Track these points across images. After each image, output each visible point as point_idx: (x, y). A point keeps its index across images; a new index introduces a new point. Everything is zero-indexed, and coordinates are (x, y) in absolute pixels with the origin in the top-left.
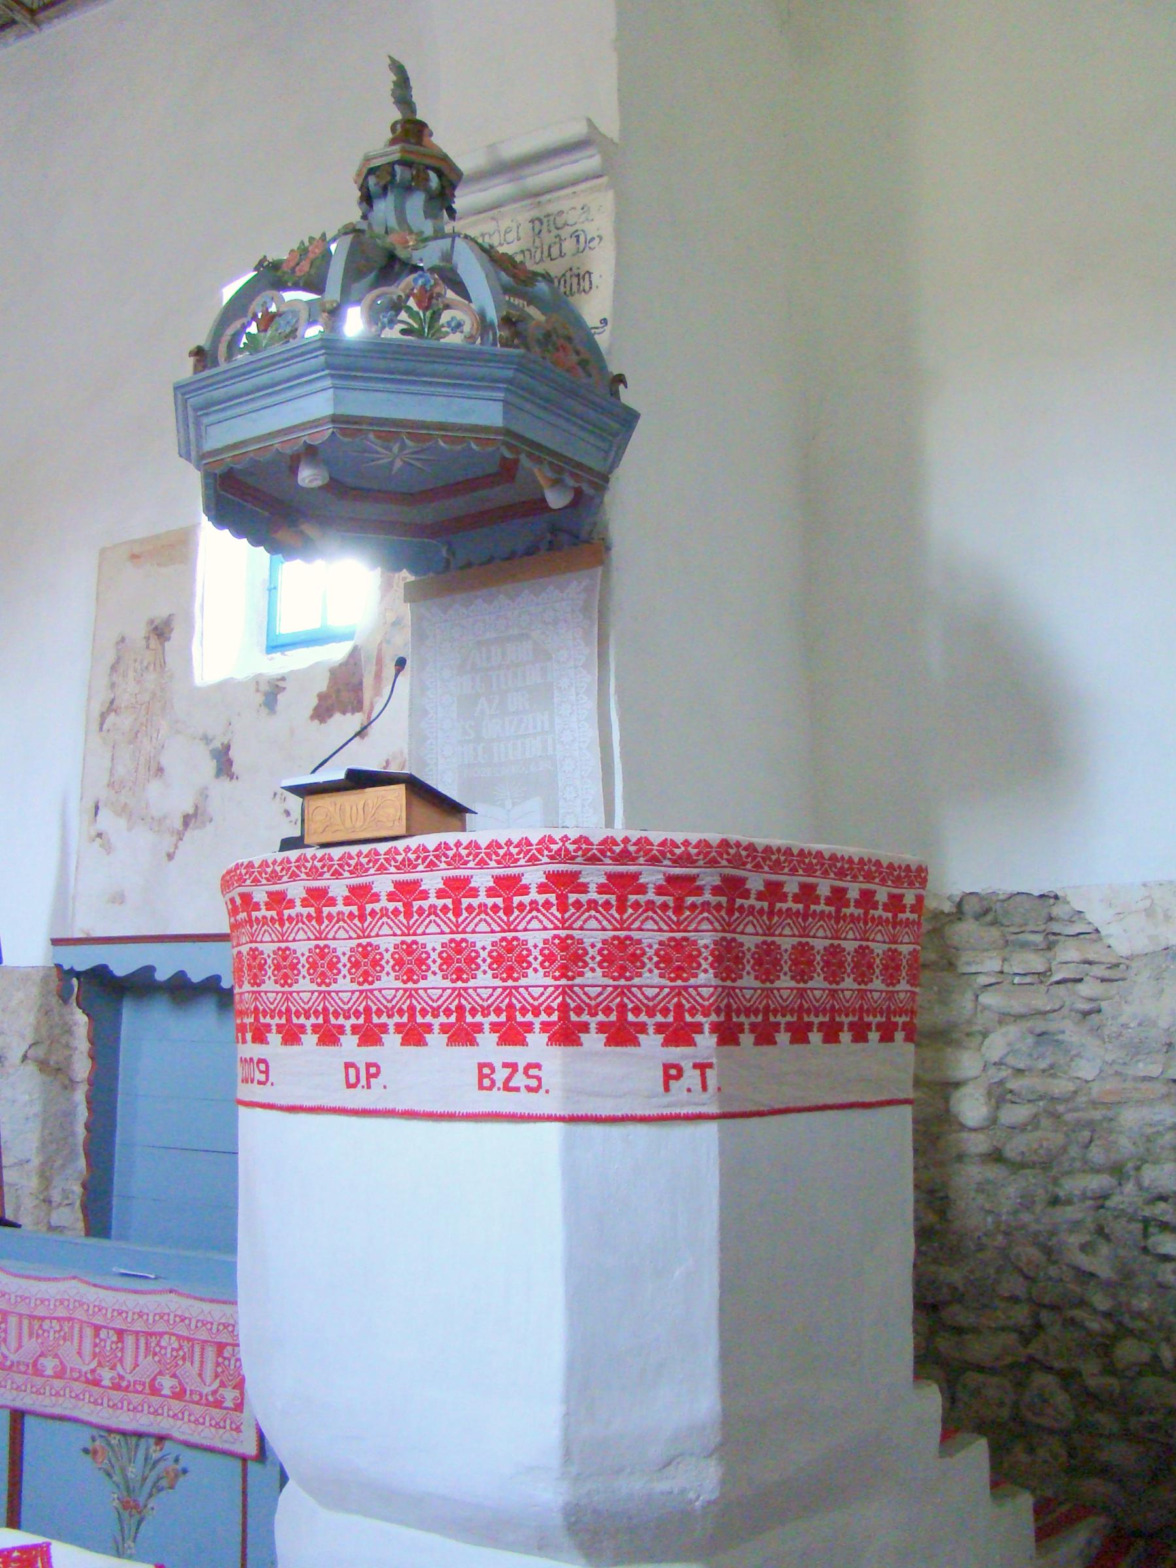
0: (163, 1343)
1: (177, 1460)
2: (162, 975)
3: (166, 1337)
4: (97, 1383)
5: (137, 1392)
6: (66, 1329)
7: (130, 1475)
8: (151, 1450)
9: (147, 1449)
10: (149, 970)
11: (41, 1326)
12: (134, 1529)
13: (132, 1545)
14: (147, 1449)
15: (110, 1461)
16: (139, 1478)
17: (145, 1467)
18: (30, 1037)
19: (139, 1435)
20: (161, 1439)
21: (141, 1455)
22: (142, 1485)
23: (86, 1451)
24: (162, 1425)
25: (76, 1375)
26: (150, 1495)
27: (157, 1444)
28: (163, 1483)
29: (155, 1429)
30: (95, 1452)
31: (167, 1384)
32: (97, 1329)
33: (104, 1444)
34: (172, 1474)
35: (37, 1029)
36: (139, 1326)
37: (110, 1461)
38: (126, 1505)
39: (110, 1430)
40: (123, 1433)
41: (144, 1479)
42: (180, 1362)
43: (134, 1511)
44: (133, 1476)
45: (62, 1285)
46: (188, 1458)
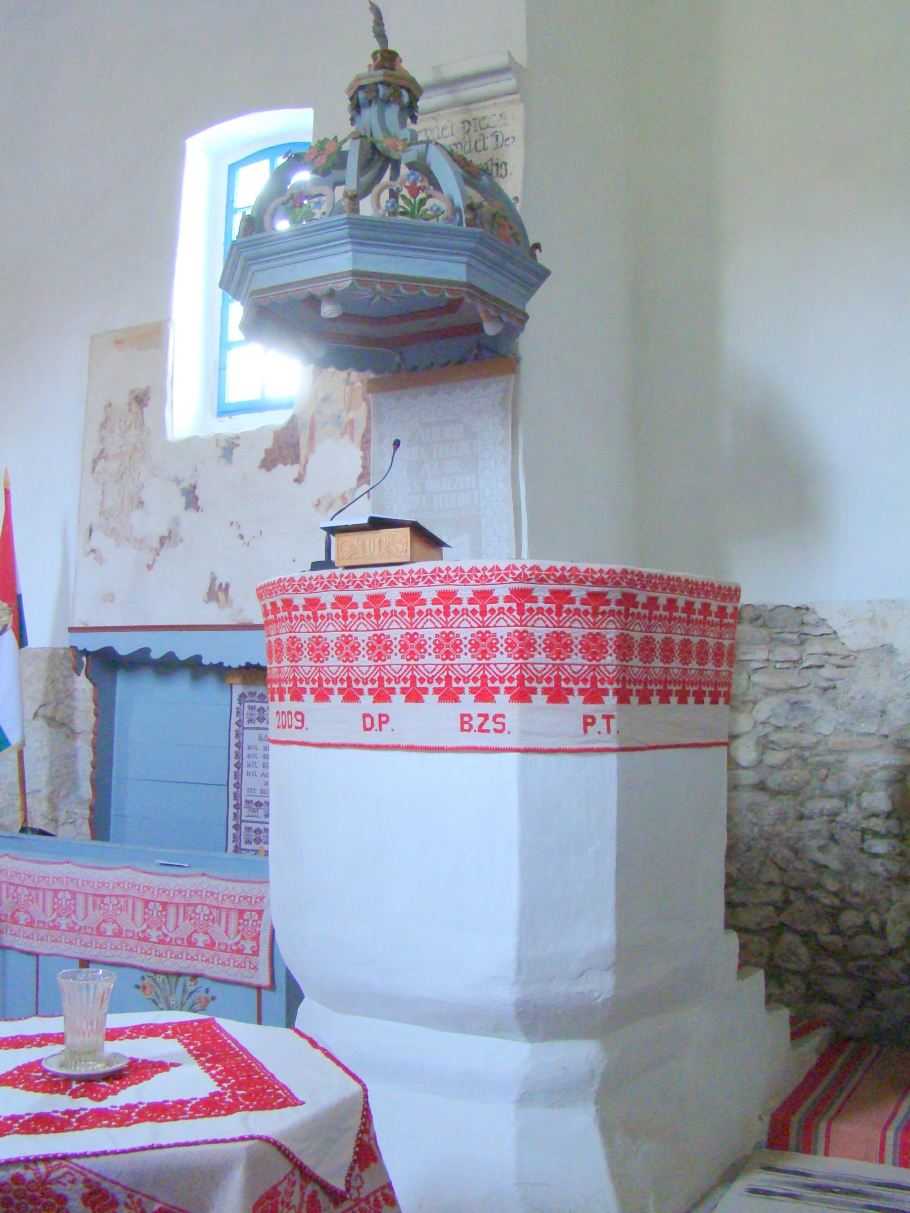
0: (197, 911)
1: (207, 991)
3: (200, 907)
4: (146, 939)
6: (122, 903)
11: (102, 902)
14: (185, 985)
15: (156, 993)
19: (179, 975)
20: (195, 977)
21: (180, 989)
23: (138, 987)
25: (130, 934)
27: (192, 980)
29: (192, 970)
30: (144, 988)
31: (201, 939)
32: (147, 902)
33: (152, 982)
34: (203, 1000)
37: (156, 993)
39: (156, 972)
40: (166, 974)
44: (174, 1003)
45: (119, 873)
46: (216, 988)
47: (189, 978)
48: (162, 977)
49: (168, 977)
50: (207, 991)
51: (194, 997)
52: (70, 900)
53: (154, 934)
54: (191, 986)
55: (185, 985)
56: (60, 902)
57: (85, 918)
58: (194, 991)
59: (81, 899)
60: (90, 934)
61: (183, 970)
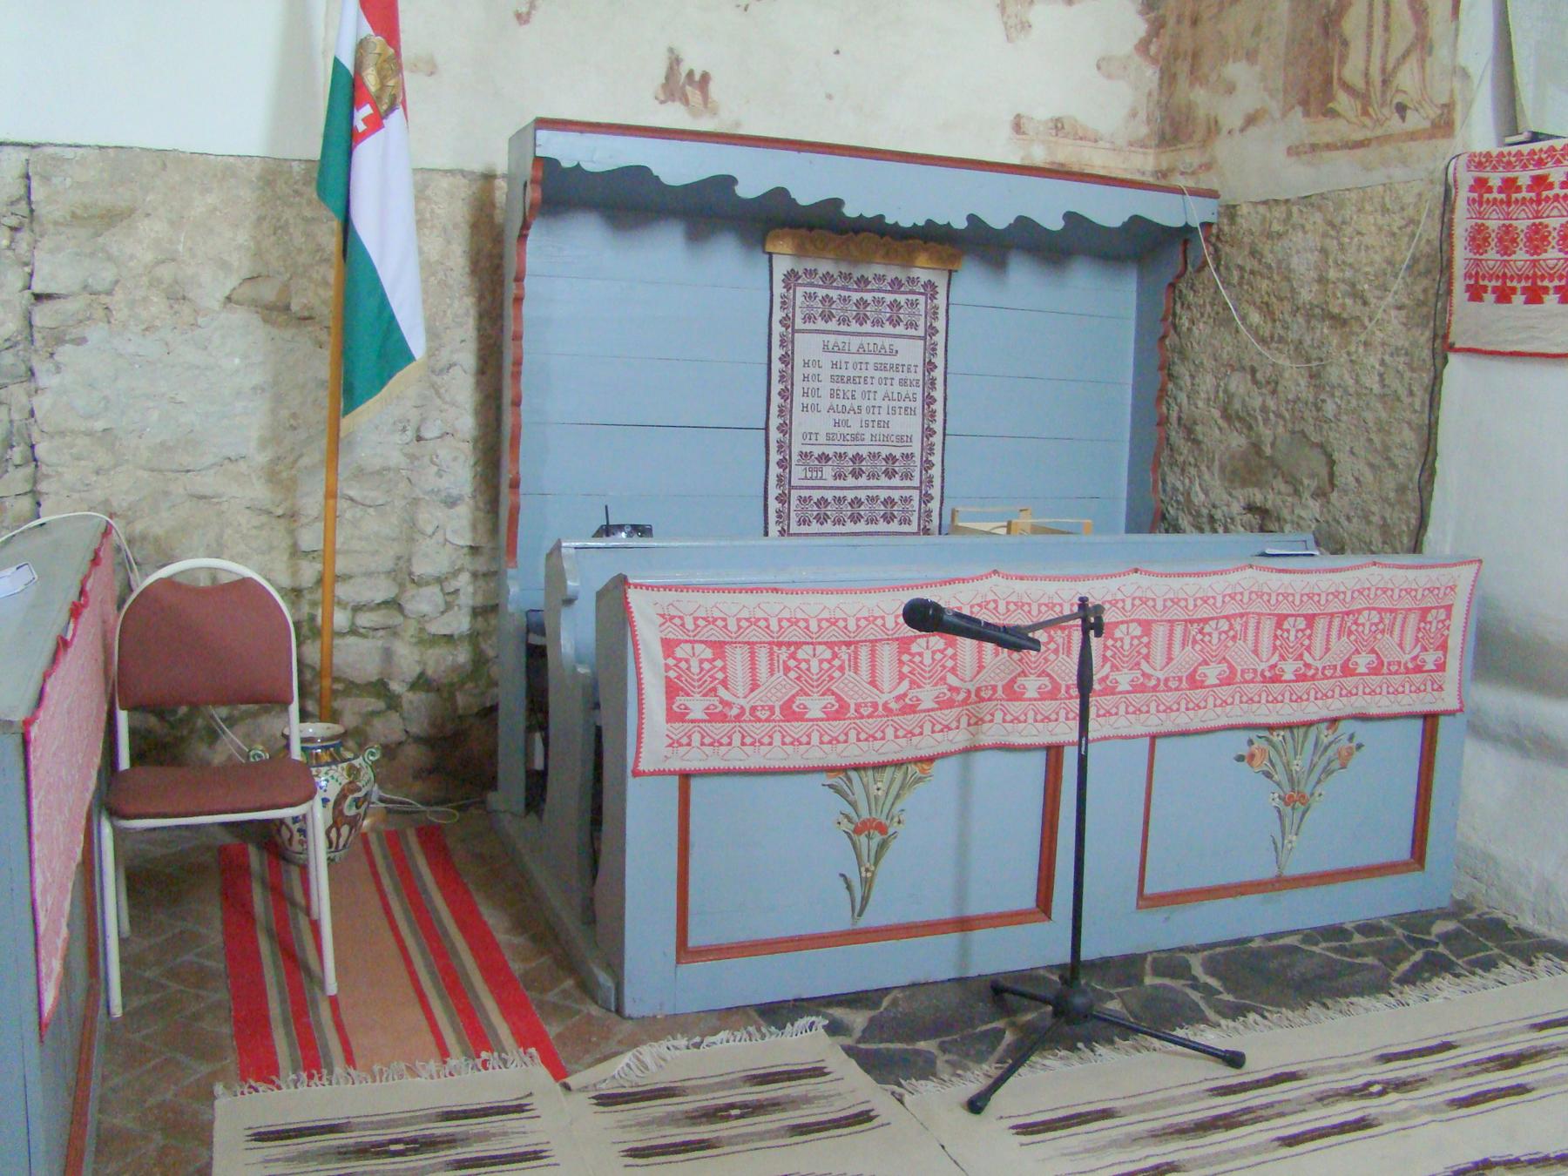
0: (1361, 620)
1: (1351, 738)
2: (748, 189)
3: (1366, 613)
4: (1276, 679)
5: (1326, 678)
7: (1294, 768)
8: (1322, 736)
9: (1319, 733)
10: (729, 182)
12: (1296, 821)
13: (1294, 838)
14: (1317, 739)
15: (1271, 761)
16: (1306, 768)
17: (1314, 753)
18: (242, 265)
20: (1334, 721)
21: (1309, 745)
22: (1309, 775)
23: (1240, 758)
24: (1356, 704)
26: (1319, 782)
28: (1336, 765)
30: (1252, 756)
31: (1363, 661)
32: (1281, 619)
33: (1263, 744)
34: (1344, 753)
35: (258, 254)
36: (1336, 606)
37: (1271, 761)
38: (1288, 801)
39: (1271, 728)
40: (1290, 727)
41: (1312, 766)
42: (1379, 636)
43: (1298, 804)
45: (1234, 578)
46: (1363, 731)
47: (1323, 726)
48: (1282, 733)
49: (1292, 732)
50: (1351, 738)
51: (1330, 753)
52: (1139, 638)
53: (1289, 669)
54: (1326, 736)
55: (1317, 739)
56: (1119, 644)
57: (1168, 664)
58: (1330, 744)
59: (1160, 631)
60: (1177, 689)
61: (1315, 717)
